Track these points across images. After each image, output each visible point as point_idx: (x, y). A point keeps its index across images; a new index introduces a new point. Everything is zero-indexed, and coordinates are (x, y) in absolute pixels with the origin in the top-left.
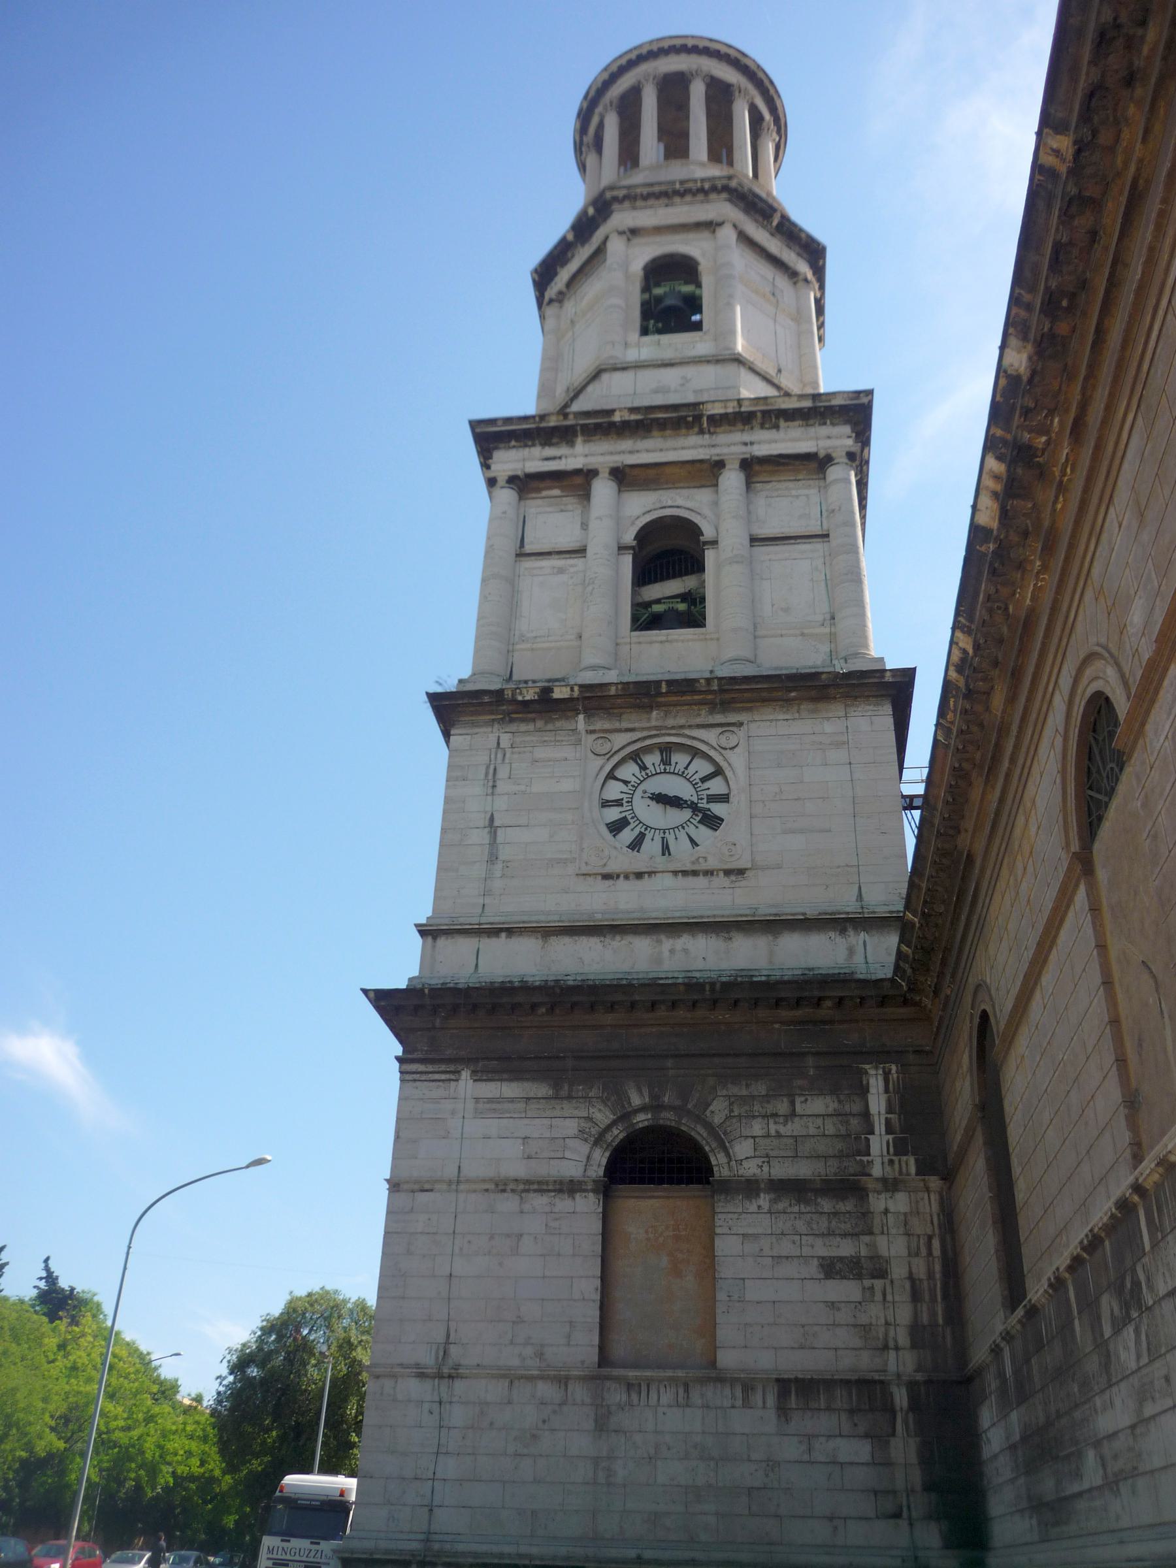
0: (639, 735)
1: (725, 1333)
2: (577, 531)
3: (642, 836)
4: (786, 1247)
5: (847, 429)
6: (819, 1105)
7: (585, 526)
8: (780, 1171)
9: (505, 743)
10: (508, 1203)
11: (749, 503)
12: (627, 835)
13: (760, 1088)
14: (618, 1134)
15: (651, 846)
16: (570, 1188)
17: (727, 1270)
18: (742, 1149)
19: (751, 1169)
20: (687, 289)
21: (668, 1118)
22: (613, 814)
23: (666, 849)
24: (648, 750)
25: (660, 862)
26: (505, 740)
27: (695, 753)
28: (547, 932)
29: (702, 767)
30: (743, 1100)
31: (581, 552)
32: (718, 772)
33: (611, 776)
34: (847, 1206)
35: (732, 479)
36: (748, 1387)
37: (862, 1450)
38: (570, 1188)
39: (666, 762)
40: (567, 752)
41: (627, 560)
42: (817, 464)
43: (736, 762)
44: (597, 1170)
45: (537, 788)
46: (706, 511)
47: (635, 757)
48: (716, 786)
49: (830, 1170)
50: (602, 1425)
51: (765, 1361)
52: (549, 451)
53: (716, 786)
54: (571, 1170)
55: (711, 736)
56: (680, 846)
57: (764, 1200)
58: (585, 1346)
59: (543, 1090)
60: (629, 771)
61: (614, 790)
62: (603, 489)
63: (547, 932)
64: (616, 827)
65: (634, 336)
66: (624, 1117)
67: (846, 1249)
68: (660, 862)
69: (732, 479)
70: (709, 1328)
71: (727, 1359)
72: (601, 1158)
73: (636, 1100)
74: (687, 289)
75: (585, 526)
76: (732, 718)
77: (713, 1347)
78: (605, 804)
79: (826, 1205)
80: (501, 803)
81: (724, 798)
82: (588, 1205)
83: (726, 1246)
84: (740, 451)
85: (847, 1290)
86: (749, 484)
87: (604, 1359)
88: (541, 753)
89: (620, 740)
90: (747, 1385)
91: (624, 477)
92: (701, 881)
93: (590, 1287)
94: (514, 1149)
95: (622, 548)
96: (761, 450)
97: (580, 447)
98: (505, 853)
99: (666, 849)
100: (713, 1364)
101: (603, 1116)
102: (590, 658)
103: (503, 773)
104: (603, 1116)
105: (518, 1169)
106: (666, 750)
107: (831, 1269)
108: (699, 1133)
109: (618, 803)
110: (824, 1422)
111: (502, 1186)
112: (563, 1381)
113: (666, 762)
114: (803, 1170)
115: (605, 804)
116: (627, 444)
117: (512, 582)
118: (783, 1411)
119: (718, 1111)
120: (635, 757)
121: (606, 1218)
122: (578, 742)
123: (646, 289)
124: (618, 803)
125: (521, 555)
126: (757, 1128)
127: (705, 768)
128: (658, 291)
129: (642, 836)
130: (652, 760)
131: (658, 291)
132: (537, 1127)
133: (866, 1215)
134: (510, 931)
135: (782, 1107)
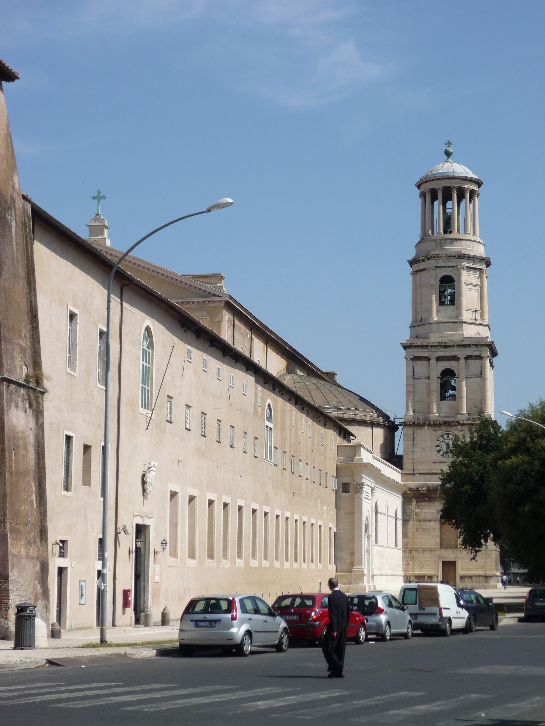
0: (442, 431)
12: (441, 453)
22: (438, 448)
24: (445, 434)
33: (438, 440)
35: (462, 361)
39: (448, 437)
47: (442, 436)
60: (441, 439)
61: (438, 443)
64: (439, 451)
69: (462, 361)
78: (436, 446)
106: (448, 434)
109: (439, 446)
113: (448, 437)
115: (436, 446)
120: (442, 436)
124: (439, 446)
130: (445, 436)
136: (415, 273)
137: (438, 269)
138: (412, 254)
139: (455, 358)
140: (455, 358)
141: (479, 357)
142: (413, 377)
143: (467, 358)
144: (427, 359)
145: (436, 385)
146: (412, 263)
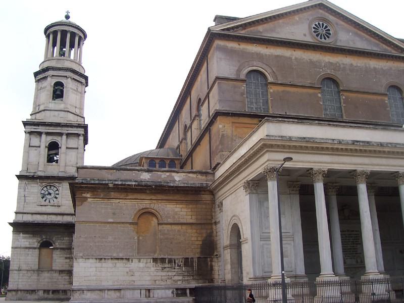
1: (53, 266)
2: (39, 143)
3: (46, 200)
4: (61, 256)
5: (83, 130)
6: (67, 238)
7: (40, 141)
8: (61, 247)
9: (27, 183)
10: (27, 250)
11: (67, 140)
12: (44, 199)
13: (59, 236)
14: (41, 242)
15: (47, 201)
16: (35, 248)
17: (54, 258)
18: (57, 244)
19: (57, 246)
20: (61, 88)
21: (48, 240)
23: (49, 202)
25: (49, 204)
26: (27, 183)
27: (54, 187)
28: (32, 214)
29: (55, 189)
30: (58, 238)
31: (39, 147)
32: (58, 190)
34: (69, 251)
35: (64, 137)
36: (56, 271)
37: (68, 277)
38: (35, 248)
40: (36, 185)
41: (47, 149)
42: (78, 135)
43: (60, 188)
44: (38, 246)
45: (32, 191)
46: (60, 141)
47: (46, 187)
48: (57, 192)
49: (67, 247)
50: (38, 276)
51: (58, 268)
52: (35, 127)
53: (57, 192)
54: (35, 246)
55: (57, 184)
56: (52, 201)
57: (59, 250)
58: (37, 267)
59: (31, 236)
60: (45, 189)
61: (43, 192)
62: (44, 136)
63: (32, 214)
65: (51, 100)
66: (42, 240)
67: (68, 256)
68: (49, 204)
69: (64, 137)
70: (51, 265)
71: (53, 268)
72: (39, 244)
73: (44, 237)
74: (61, 88)
75: (40, 141)
76: (62, 182)
77: (52, 267)
79: (67, 251)
80: (26, 193)
81: (58, 194)
82: (37, 251)
83: (54, 255)
84: (67, 132)
85: (68, 260)
86: (67, 137)
87: (39, 268)
88: (32, 185)
89: (44, 184)
90: (56, 271)
91: (48, 134)
92: (54, 207)
93: (37, 260)
94: (28, 243)
95: (46, 147)
96: (69, 132)
97: (40, 127)
98: (27, 201)
99: (49, 202)
100: (52, 269)
101: (39, 239)
102: (40, 169)
103: (26, 188)
104: (39, 239)
105: (28, 246)
107: (66, 258)
108: (51, 242)
110: (64, 275)
111: (26, 248)
112: (34, 271)
114: (64, 247)
116: (47, 128)
117: (28, 153)
118: (59, 274)
119: (54, 239)
120: (46, 187)
121: (39, 252)
122: (38, 184)
123: (54, 88)
125: (30, 146)
126: (59, 241)
127: (55, 189)
128: (56, 88)
129: (46, 200)
130: (48, 187)
131: (56, 88)
132: (31, 240)
133: (71, 252)
134: (28, 213)
135: (62, 239)
136: (38, 81)
137: (53, 77)
138: (38, 69)
139: (61, 134)
140: (61, 134)
141: (78, 135)
142: (29, 146)
143: (68, 135)
144: (40, 134)
145: (44, 152)
146: (36, 74)
